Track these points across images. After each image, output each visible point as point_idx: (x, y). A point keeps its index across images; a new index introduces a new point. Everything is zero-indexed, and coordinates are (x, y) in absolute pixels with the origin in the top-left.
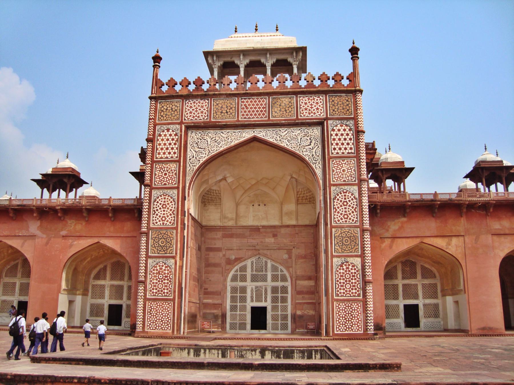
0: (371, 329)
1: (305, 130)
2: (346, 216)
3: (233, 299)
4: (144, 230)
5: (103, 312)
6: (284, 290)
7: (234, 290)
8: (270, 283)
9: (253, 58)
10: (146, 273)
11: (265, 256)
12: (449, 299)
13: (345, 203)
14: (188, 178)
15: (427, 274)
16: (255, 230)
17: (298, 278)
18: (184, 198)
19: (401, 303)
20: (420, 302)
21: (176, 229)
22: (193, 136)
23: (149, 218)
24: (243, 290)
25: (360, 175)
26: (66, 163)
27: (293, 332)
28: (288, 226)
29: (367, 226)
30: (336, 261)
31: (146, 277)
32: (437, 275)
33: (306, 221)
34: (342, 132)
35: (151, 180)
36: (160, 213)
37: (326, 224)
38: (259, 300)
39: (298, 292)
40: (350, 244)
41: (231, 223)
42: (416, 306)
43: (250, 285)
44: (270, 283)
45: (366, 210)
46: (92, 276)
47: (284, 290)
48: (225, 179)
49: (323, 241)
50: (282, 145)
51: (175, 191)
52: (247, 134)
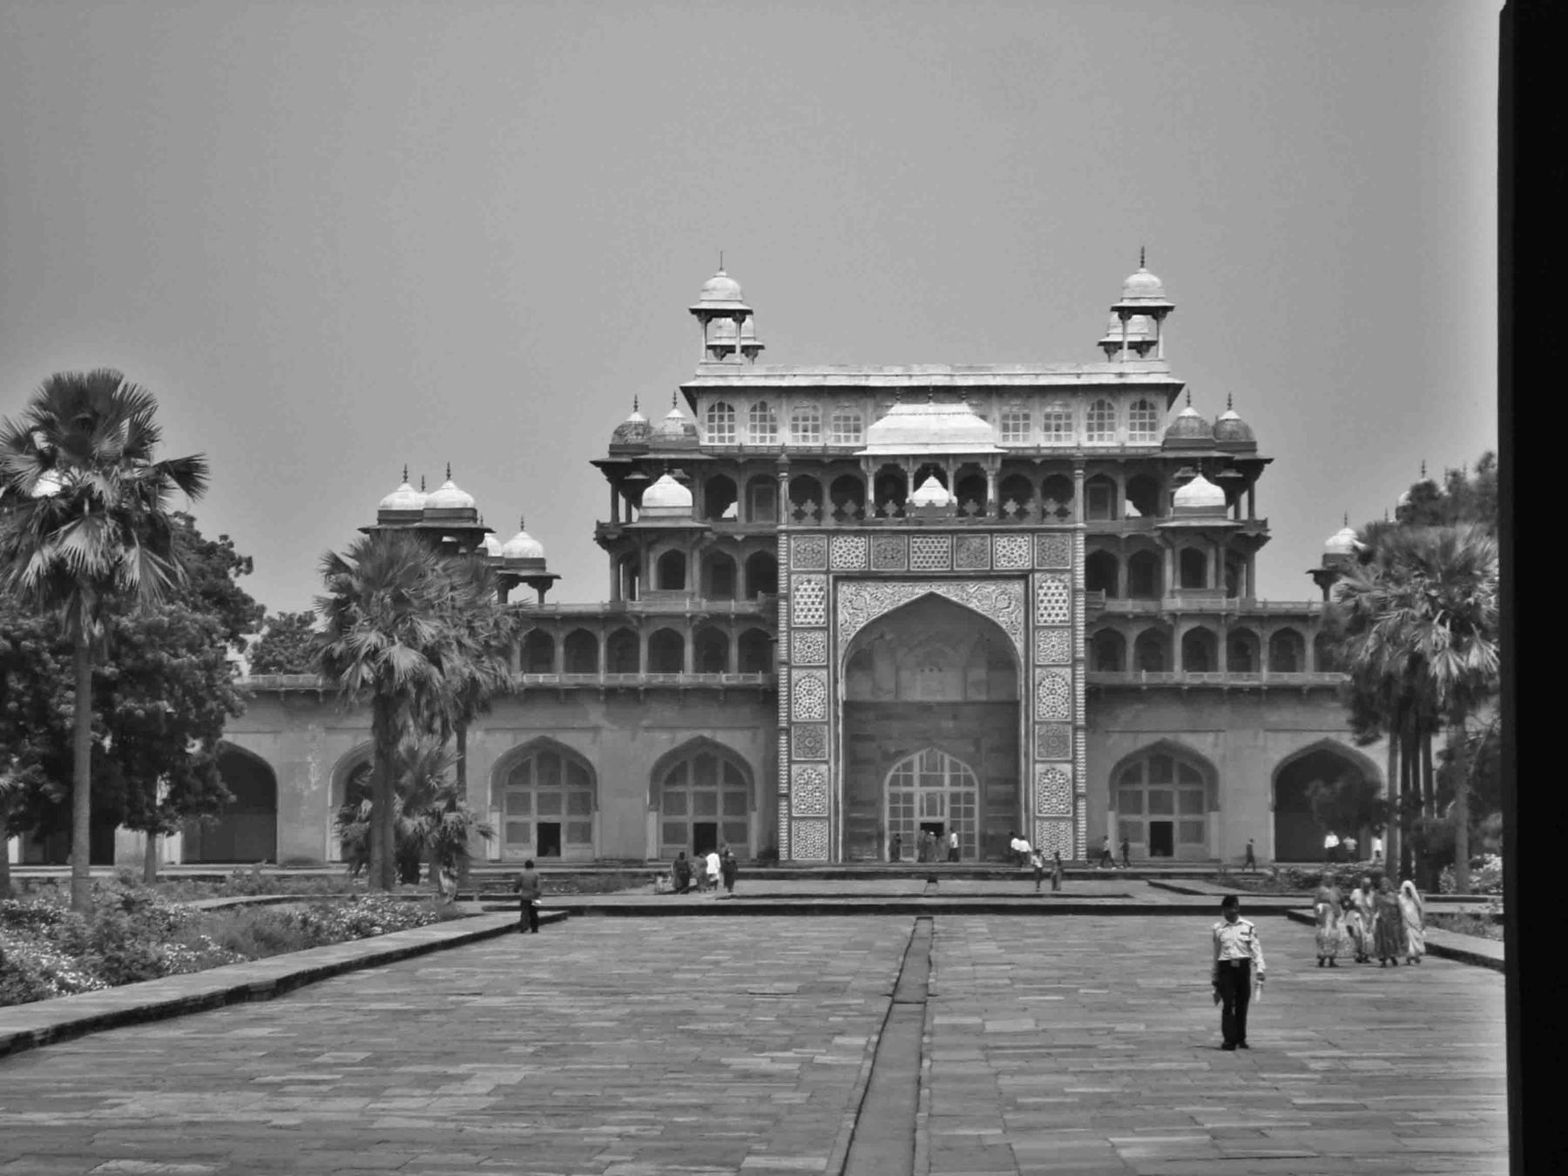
0: (1082, 853)
1: (1003, 585)
2: (1054, 708)
3: (894, 811)
4: (784, 725)
5: (685, 835)
6: (969, 798)
7: (895, 798)
8: (947, 788)
9: (928, 461)
10: (789, 783)
11: (940, 748)
12: (1214, 816)
13: (1052, 692)
14: (841, 652)
15: (1189, 776)
16: (925, 708)
17: (991, 781)
18: (836, 681)
19: (1146, 819)
20: (1175, 818)
21: (828, 723)
22: (846, 590)
23: (789, 708)
24: (909, 798)
25: (1074, 652)
26: (450, 495)
27: (983, 858)
28: (974, 703)
29: (1081, 722)
30: (1039, 768)
31: (789, 788)
32: (1205, 780)
33: (1001, 695)
34: (1053, 590)
35: (789, 654)
36: (805, 701)
37: (1027, 719)
38: (931, 812)
39: (988, 802)
40: (1057, 745)
41: (887, 698)
42: (1167, 827)
43: (918, 791)
44: (947, 788)
45: (1081, 700)
46: (665, 776)
47: (969, 798)
48: (882, 636)
49: (1023, 741)
50: (971, 606)
51: (825, 672)
52: (921, 590)
